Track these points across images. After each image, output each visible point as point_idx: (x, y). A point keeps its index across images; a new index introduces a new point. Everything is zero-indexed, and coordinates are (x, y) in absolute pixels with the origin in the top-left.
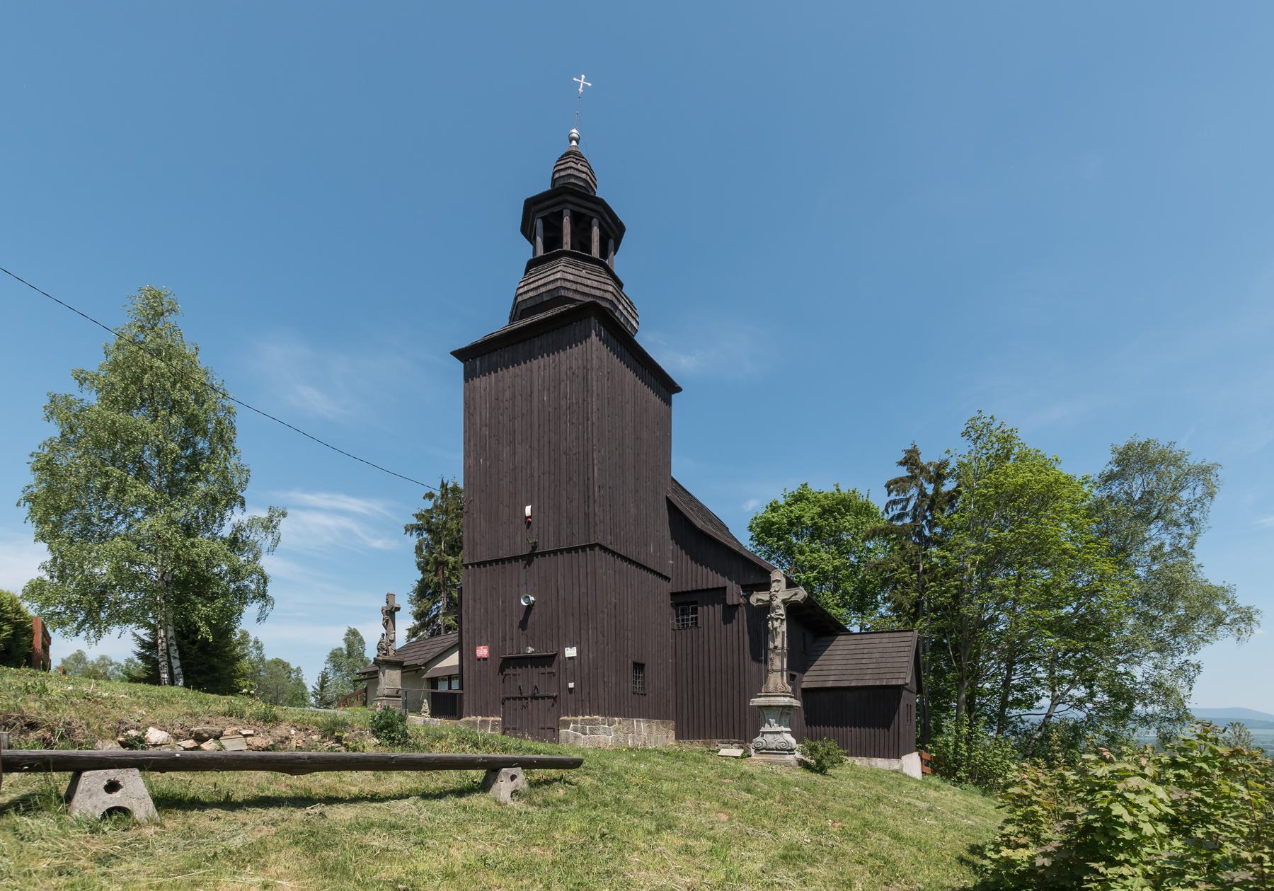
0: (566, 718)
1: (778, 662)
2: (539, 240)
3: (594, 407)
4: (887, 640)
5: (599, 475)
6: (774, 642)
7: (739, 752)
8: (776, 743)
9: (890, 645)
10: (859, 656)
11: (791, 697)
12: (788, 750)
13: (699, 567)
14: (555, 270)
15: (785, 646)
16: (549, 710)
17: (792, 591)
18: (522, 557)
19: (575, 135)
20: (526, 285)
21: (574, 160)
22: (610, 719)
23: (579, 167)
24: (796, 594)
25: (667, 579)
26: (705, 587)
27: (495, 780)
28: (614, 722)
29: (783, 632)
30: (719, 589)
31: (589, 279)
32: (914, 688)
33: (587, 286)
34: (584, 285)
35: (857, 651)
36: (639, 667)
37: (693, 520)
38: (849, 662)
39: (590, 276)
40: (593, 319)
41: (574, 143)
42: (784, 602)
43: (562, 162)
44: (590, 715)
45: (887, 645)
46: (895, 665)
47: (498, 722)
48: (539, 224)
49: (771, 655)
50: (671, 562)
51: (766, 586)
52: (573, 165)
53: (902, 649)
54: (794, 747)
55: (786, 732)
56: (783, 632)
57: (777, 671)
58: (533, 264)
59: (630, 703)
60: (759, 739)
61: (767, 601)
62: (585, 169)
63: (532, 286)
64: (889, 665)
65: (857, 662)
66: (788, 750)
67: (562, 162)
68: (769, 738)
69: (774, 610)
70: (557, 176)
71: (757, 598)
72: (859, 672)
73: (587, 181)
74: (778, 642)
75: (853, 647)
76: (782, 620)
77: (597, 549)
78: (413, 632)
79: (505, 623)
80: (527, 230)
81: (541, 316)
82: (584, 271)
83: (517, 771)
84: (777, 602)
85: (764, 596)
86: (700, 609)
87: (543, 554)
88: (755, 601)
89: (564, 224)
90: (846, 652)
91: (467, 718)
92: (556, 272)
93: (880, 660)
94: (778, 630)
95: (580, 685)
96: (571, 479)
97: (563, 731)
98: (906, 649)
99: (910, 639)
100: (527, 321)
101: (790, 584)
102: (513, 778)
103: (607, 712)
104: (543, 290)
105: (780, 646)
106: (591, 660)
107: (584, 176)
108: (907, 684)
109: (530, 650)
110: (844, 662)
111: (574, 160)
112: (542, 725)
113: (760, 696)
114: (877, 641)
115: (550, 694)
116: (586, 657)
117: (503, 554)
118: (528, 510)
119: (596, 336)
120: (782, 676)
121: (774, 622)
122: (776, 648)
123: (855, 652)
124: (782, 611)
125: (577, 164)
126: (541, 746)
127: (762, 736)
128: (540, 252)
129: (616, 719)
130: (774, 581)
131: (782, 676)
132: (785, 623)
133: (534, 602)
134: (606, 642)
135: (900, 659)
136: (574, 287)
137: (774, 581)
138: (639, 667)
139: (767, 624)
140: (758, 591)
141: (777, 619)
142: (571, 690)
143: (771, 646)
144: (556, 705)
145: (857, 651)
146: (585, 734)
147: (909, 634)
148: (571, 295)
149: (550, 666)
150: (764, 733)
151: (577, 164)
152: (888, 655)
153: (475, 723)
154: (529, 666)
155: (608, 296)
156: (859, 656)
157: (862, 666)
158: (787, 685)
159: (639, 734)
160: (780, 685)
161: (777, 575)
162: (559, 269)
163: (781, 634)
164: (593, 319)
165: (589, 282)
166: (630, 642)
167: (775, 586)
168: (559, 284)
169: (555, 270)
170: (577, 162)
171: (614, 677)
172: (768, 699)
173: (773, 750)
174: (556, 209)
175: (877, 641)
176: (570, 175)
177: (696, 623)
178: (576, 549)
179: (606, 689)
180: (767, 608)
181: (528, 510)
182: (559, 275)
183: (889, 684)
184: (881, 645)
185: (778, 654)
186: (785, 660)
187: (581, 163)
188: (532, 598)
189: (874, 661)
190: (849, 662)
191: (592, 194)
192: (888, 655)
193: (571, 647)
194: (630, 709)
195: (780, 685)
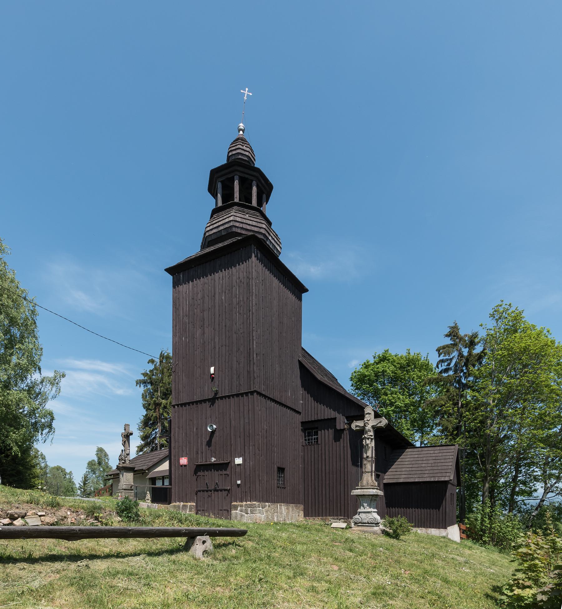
0: (235, 503)
1: (369, 466)
2: (219, 196)
3: (254, 303)
4: (438, 451)
5: (256, 346)
6: (366, 453)
7: (344, 525)
8: (368, 519)
9: (440, 455)
10: (420, 462)
11: (377, 489)
12: (376, 524)
13: (319, 405)
14: (230, 215)
15: (374, 456)
16: (225, 498)
17: (378, 420)
18: (209, 400)
19: (242, 127)
20: (211, 225)
21: (241, 144)
22: (263, 504)
23: (244, 148)
25: (299, 413)
26: (322, 418)
27: (193, 543)
28: (265, 506)
29: (373, 447)
30: (332, 419)
31: (250, 220)
32: (456, 482)
33: (249, 225)
34: (247, 224)
35: (419, 459)
36: (281, 470)
37: (315, 375)
38: (414, 466)
39: (251, 219)
40: (253, 246)
41: (241, 132)
42: (373, 427)
43: (234, 145)
44: (251, 502)
45: (438, 455)
46: (443, 468)
47: (193, 506)
48: (219, 185)
49: (365, 462)
50: (301, 402)
51: (361, 417)
52: (240, 146)
53: (448, 457)
54: (379, 522)
55: (374, 512)
56: (373, 447)
57: (368, 472)
58: (215, 211)
59: (276, 493)
60: (357, 516)
61: (362, 427)
62: (248, 149)
63: (215, 225)
64: (440, 468)
65: (419, 466)
66: (376, 524)
67: (234, 145)
68: (363, 516)
69: (366, 433)
70: (230, 154)
71: (356, 425)
72: (420, 472)
73: (250, 157)
74: (369, 453)
75: (416, 456)
76: (372, 439)
77: (255, 394)
78: (141, 449)
79: (198, 443)
80: (212, 190)
81: (220, 245)
82: (247, 215)
83: (207, 538)
84: (369, 427)
85: (360, 423)
86: (319, 432)
87: (221, 398)
89: (235, 185)
90: (412, 459)
91: (174, 504)
92: (230, 216)
93: (433, 465)
94: (369, 445)
95: (244, 482)
96: (239, 349)
97: (233, 512)
98: (451, 457)
99: (453, 450)
100: (212, 248)
101: (377, 416)
102: (204, 542)
103: (261, 499)
104: (222, 228)
105: (370, 456)
106: (251, 466)
107: (247, 154)
108: (451, 480)
109: (213, 459)
110: (411, 466)
111: (241, 144)
112: (220, 508)
113: (358, 489)
114: (432, 452)
115: (226, 488)
116: (248, 464)
117: (196, 398)
118: (212, 370)
119: (255, 257)
120: (372, 475)
121: (367, 440)
122: (368, 457)
123: (417, 459)
124: (372, 433)
125: (243, 146)
126: (220, 522)
127: (359, 515)
128: (220, 204)
129: (267, 504)
130: (367, 414)
131: (372, 475)
132: (373, 441)
133: (216, 428)
134: (260, 455)
135: (446, 464)
136: (241, 225)
137: (367, 414)
138: (281, 470)
139: (362, 442)
140: (357, 420)
142: (238, 485)
143: (365, 456)
144: (229, 495)
145: (419, 459)
146: (247, 514)
147: (452, 447)
148: (239, 231)
149: (226, 470)
150: (360, 513)
151: (243, 146)
152: (439, 461)
153: (179, 506)
154: (213, 470)
155: (263, 231)
156: (420, 462)
157: (422, 469)
158: (374, 481)
159: (281, 513)
160: (370, 481)
161: (369, 410)
162: (232, 214)
163: (371, 449)
164: (253, 246)
165: (250, 223)
166: (275, 454)
167: (367, 417)
168: (231, 224)
169: (230, 215)
170: (243, 145)
171: (265, 477)
172: (363, 490)
173: (366, 523)
174: (230, 176)
175: (432, 452)
176: (239, 153)
177: (317, 442)
178: (242, 394)
179: (261, 485)
180: (362, 431)
181: (212, 370)
182: (231, 218)
183: (440, 480)
184: (434, 455)
185: (369, 461)
186: (374, 465)
187: (246, 145)
188: (215, 426)
189: (430, 465)
190: (414, 466)
191: (253, 165)
192: (439, 461)
193: (239, 457)
194: (276, 498)
195: (370, 481)
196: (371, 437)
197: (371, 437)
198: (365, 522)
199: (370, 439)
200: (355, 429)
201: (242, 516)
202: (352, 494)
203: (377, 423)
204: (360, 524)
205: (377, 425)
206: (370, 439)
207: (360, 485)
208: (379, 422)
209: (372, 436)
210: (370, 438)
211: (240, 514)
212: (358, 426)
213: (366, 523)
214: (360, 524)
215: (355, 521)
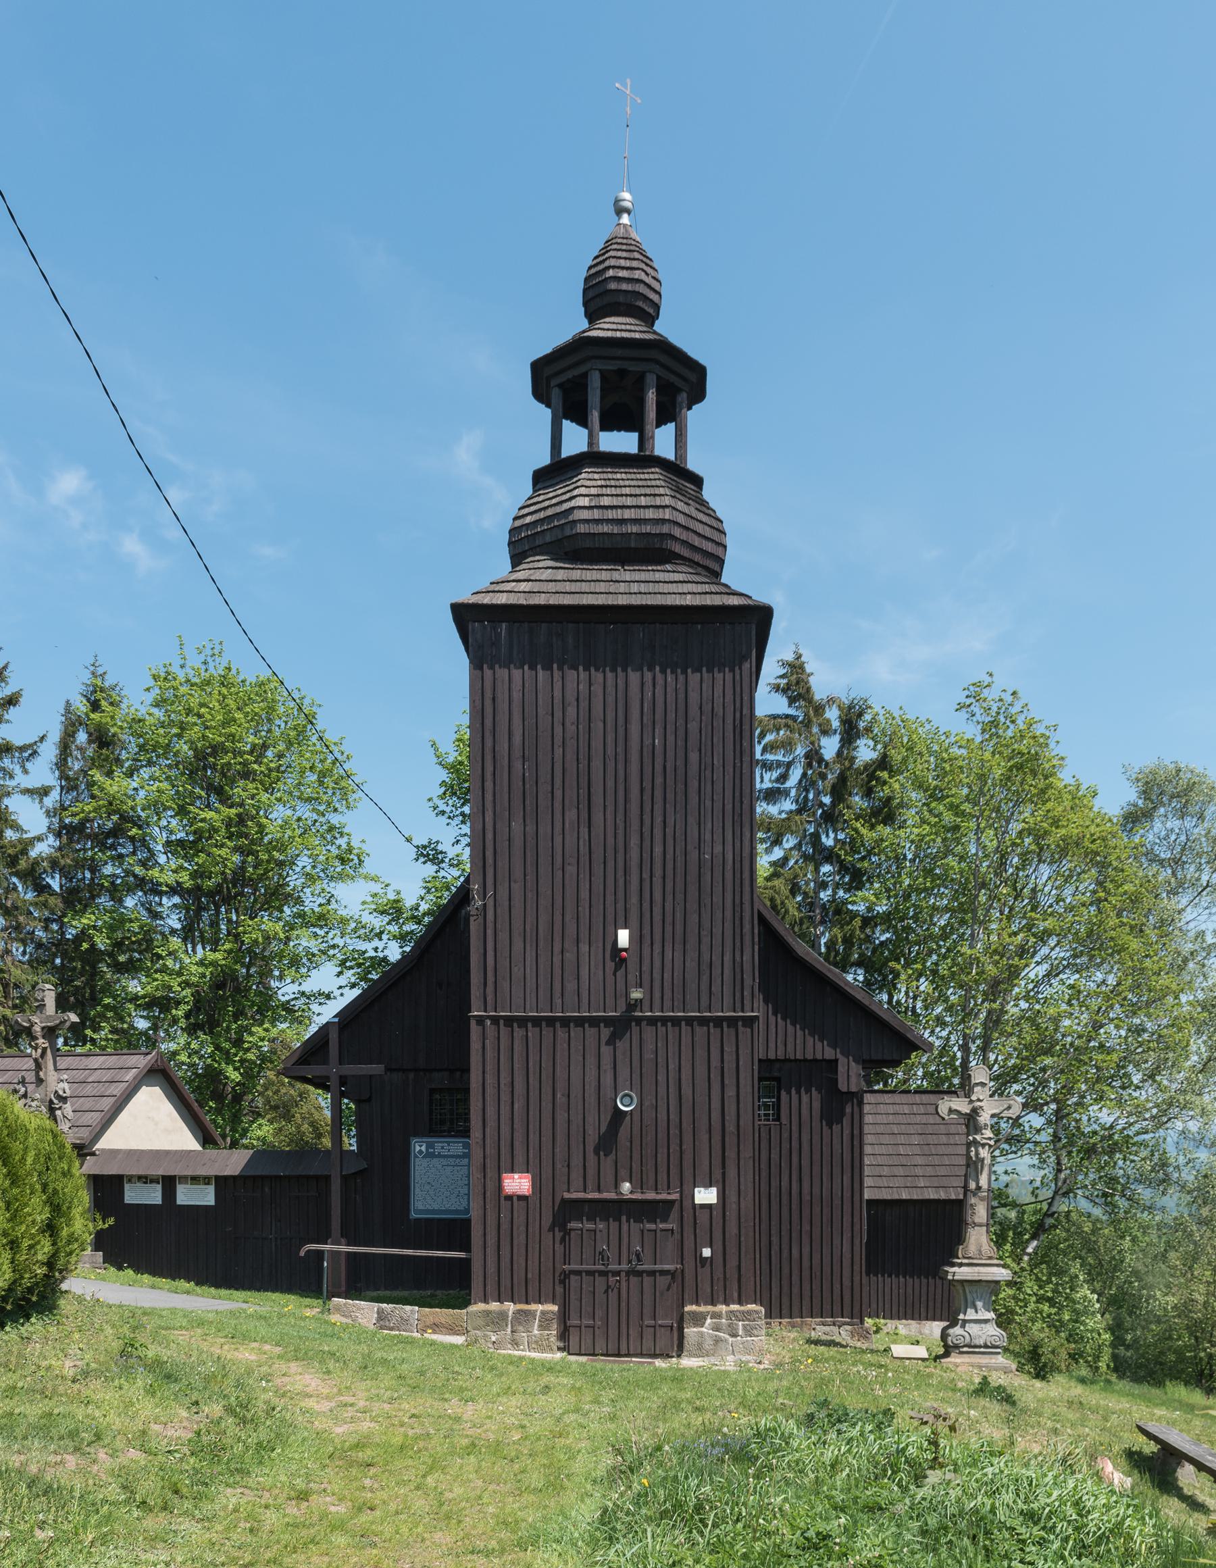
8: (984, 1337)
24: (1009, 1108)
44: (740, 1303)
49: (973, 1200)
57: (980, 1225)
68: (973, 1329)
88: (946, 1112)
113: (961, 1265)
121: (980, 1149)
127: (963, 1326)
137: (977, 1084)
141: (983, 1145)
146: (734, 1335)
150: (965, 1322)
173: (980, 1347)
185: (982, 1199)
201: (717, 1341)
202: (950, 1277)
204: (965, 1349)
209: (990, 1139)
211: (711, 1336)
213: (980, 1347)
214: (965, 1349)
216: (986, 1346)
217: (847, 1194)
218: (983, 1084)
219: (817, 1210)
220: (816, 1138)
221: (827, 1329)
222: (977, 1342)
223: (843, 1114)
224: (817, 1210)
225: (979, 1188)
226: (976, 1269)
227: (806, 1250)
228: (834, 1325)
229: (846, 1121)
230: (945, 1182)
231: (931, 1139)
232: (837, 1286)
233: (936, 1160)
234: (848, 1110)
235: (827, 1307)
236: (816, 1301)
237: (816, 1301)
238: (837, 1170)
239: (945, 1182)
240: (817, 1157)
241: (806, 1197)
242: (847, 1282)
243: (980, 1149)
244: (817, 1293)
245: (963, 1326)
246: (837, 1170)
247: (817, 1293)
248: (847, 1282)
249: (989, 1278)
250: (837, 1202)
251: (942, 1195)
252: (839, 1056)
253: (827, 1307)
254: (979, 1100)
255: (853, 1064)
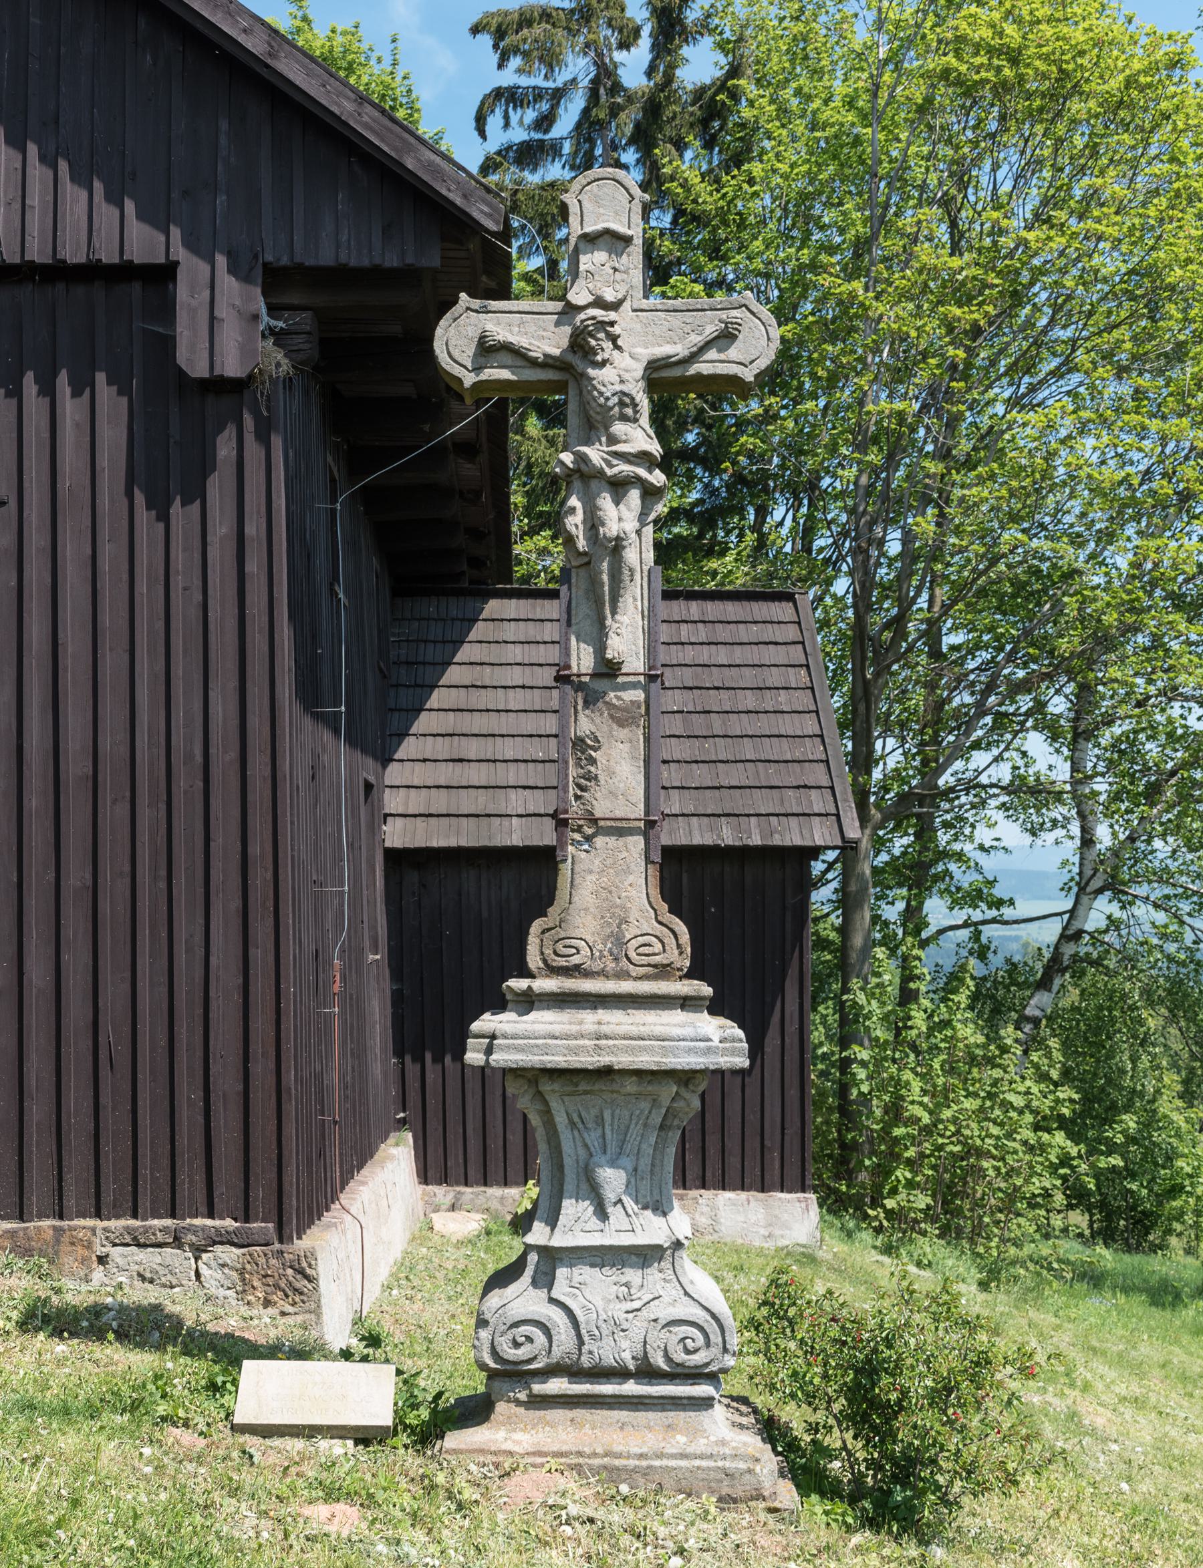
8: (638, 1328)
24: (726, 336)
61: (549, 363)
88: (466, 353)
113: (528, 1002)
127: (544, 1279)
137: (591, 240)
141: (619, 487)
185: (623, 718)
196: (642, 472)
197: (642, 472)
198: (609, 1360)
199: (634, 495)
200: (469, 379)
202: (474, 1057)
203: (697, 339)
204: (557, 1386)
205: (693, 358)
206: (634, 495)
207: (533, 960)
208: (710, 330)
210: (639, 480)
212: (507, 348)
213: (620, 1373)
214: (557, 1386)
215: (510, 1353)
216: (647, 1372)
217: (224, 757)
218: (615, 241)
219: (114, 813)
220: (111, 552)
221: (149, 1258)
222: (606, 1352)
223: (205, 465)
224: (114, 813)
225: (609, 670)
226: (589, 1019)
227: (76, 960)
228: (177, 1242)
229: (218, 487)
230: (737, 802)
231: (713, 700)
232: (189, 1094)
233: (722, 750)
234: (225, 448)
235: (152, 1174)
236: (114, 1151)
237: (114, 1151)
238: (185, 667)
239: (737, 802)
240: (112, 617)
241: (76, 766)
242: (226, 1081)
243: (606, 502)
244: (115, 1119)
245: (544, 1279)
246: (185, 667)
247: (115, 1119)
248: (226, 1081)
249: (646, 1061)
250: (186, 782)
251: (727, 835)
252: (180, 253)
253: (152, 1174)
254: (599, 303)
255: (228, 284)
